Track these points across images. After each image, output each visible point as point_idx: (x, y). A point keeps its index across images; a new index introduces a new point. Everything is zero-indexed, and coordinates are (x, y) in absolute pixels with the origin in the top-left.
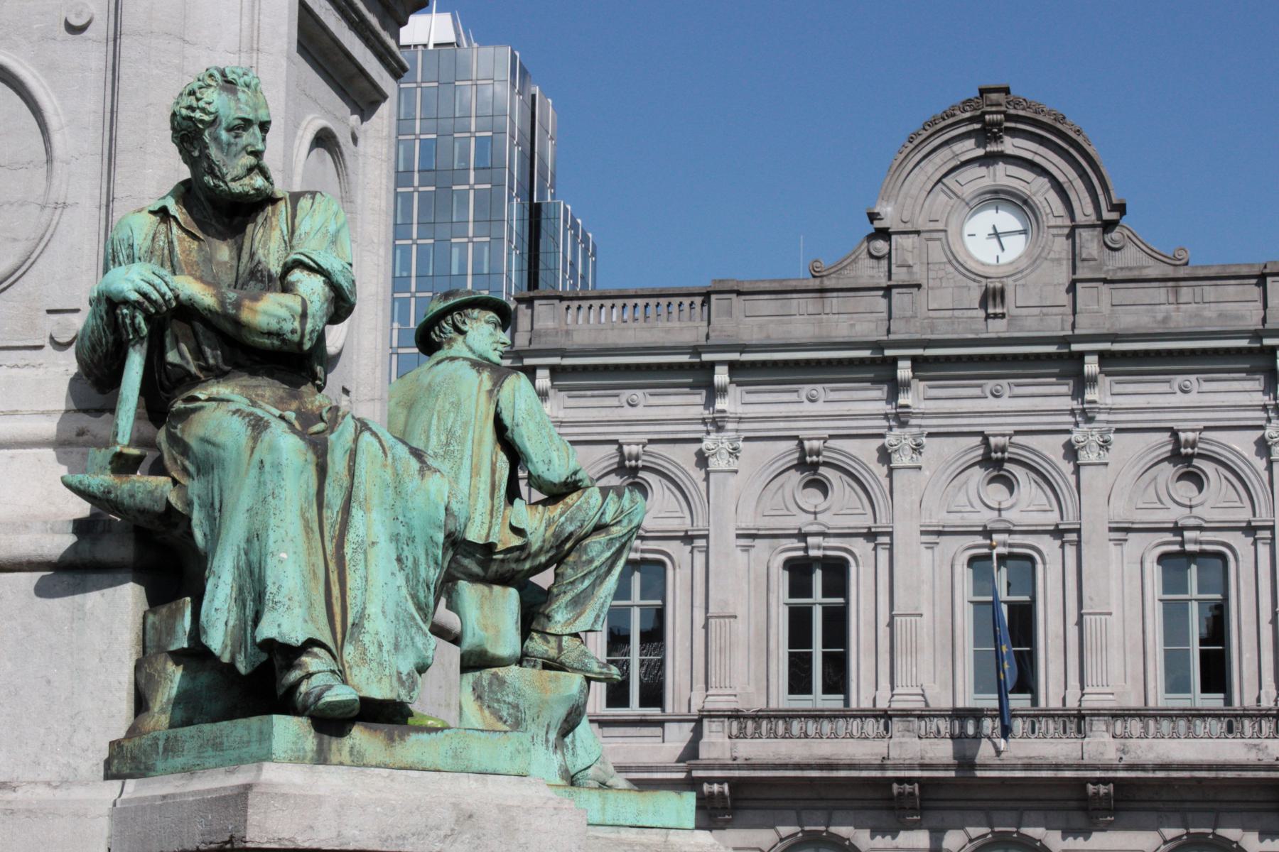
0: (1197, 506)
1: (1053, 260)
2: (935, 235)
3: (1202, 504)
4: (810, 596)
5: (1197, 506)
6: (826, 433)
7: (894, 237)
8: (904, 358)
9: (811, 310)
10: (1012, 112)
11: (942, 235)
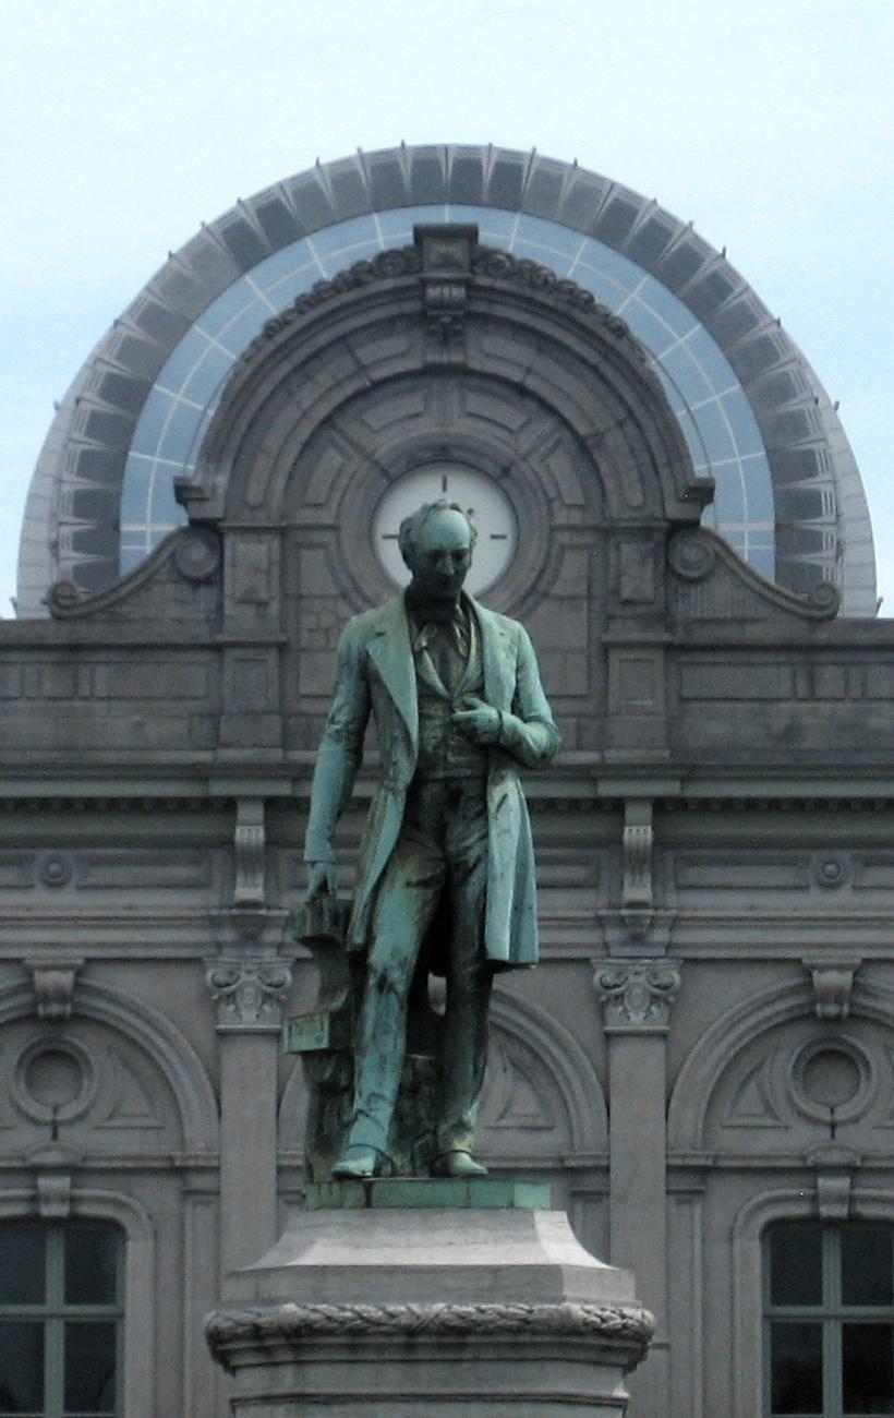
0: (845, 1123)
1: (562, 599)
2: (317, 537)
3: (856, 1120)
4: (41, 1300)
5: (845, 1123)
6: (78, 956)
7: (229, 541)
8: (252, 799)
9: (49, 687)
10: (483, 281)
11: (328, 537)
